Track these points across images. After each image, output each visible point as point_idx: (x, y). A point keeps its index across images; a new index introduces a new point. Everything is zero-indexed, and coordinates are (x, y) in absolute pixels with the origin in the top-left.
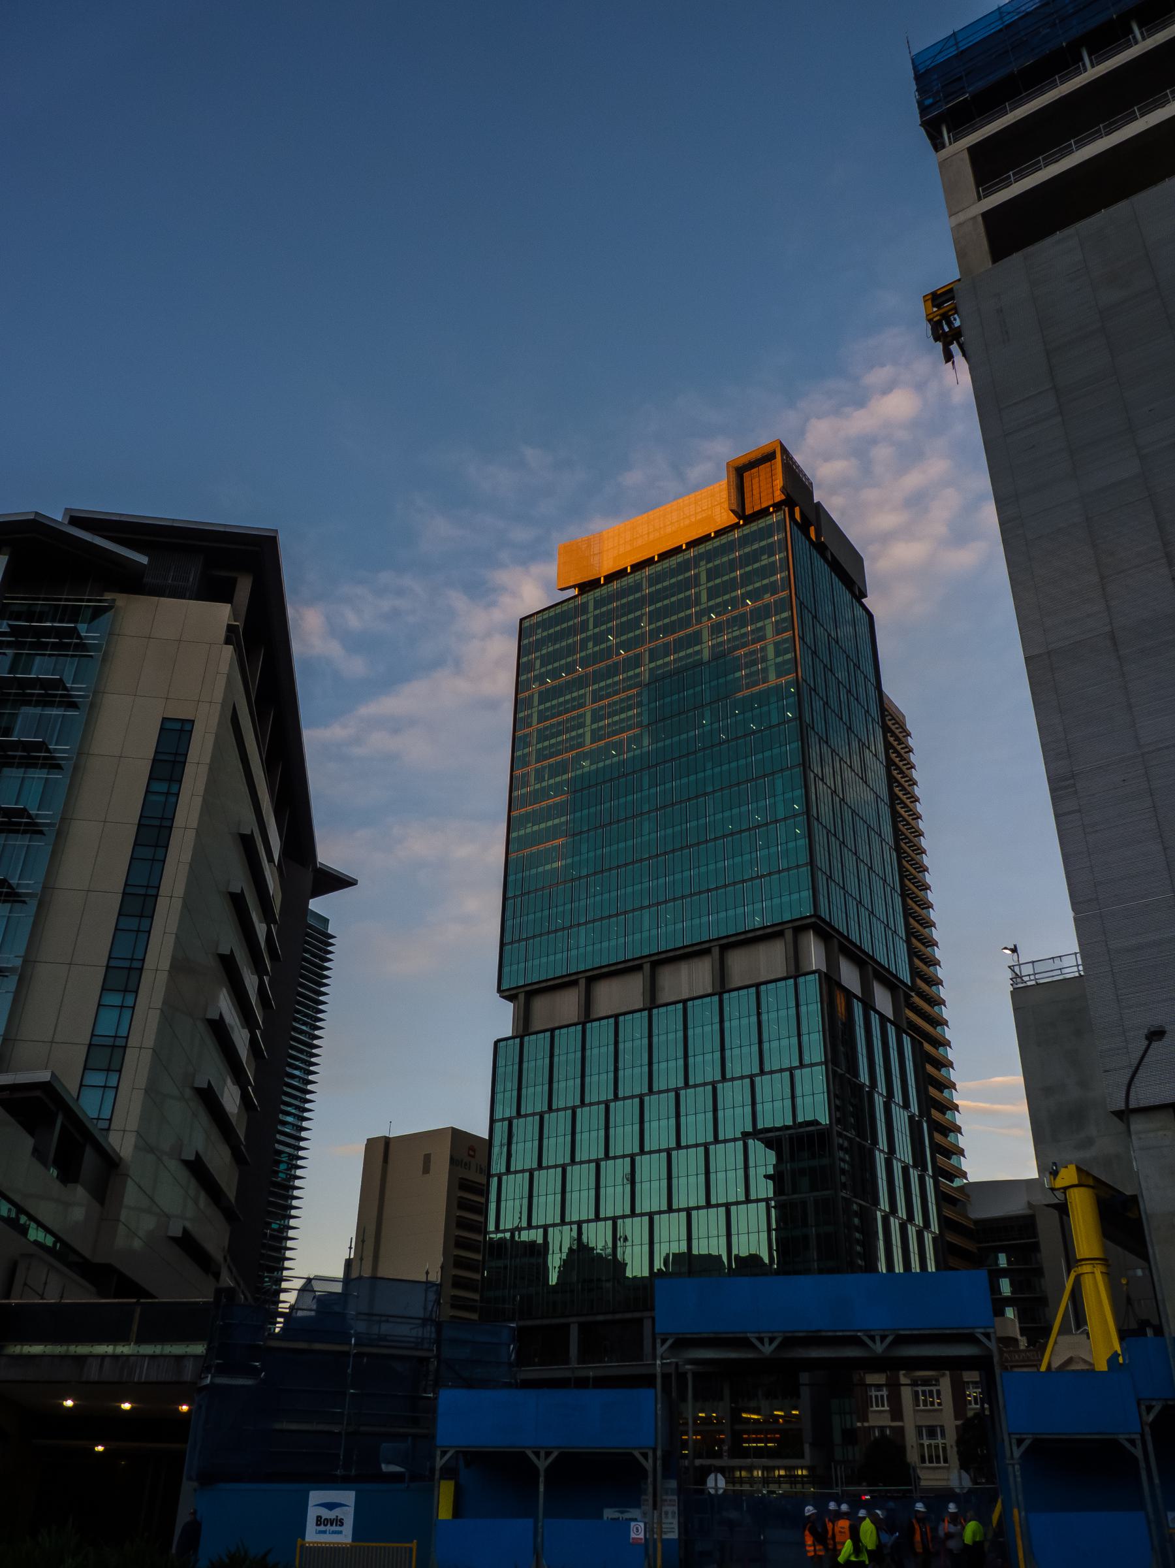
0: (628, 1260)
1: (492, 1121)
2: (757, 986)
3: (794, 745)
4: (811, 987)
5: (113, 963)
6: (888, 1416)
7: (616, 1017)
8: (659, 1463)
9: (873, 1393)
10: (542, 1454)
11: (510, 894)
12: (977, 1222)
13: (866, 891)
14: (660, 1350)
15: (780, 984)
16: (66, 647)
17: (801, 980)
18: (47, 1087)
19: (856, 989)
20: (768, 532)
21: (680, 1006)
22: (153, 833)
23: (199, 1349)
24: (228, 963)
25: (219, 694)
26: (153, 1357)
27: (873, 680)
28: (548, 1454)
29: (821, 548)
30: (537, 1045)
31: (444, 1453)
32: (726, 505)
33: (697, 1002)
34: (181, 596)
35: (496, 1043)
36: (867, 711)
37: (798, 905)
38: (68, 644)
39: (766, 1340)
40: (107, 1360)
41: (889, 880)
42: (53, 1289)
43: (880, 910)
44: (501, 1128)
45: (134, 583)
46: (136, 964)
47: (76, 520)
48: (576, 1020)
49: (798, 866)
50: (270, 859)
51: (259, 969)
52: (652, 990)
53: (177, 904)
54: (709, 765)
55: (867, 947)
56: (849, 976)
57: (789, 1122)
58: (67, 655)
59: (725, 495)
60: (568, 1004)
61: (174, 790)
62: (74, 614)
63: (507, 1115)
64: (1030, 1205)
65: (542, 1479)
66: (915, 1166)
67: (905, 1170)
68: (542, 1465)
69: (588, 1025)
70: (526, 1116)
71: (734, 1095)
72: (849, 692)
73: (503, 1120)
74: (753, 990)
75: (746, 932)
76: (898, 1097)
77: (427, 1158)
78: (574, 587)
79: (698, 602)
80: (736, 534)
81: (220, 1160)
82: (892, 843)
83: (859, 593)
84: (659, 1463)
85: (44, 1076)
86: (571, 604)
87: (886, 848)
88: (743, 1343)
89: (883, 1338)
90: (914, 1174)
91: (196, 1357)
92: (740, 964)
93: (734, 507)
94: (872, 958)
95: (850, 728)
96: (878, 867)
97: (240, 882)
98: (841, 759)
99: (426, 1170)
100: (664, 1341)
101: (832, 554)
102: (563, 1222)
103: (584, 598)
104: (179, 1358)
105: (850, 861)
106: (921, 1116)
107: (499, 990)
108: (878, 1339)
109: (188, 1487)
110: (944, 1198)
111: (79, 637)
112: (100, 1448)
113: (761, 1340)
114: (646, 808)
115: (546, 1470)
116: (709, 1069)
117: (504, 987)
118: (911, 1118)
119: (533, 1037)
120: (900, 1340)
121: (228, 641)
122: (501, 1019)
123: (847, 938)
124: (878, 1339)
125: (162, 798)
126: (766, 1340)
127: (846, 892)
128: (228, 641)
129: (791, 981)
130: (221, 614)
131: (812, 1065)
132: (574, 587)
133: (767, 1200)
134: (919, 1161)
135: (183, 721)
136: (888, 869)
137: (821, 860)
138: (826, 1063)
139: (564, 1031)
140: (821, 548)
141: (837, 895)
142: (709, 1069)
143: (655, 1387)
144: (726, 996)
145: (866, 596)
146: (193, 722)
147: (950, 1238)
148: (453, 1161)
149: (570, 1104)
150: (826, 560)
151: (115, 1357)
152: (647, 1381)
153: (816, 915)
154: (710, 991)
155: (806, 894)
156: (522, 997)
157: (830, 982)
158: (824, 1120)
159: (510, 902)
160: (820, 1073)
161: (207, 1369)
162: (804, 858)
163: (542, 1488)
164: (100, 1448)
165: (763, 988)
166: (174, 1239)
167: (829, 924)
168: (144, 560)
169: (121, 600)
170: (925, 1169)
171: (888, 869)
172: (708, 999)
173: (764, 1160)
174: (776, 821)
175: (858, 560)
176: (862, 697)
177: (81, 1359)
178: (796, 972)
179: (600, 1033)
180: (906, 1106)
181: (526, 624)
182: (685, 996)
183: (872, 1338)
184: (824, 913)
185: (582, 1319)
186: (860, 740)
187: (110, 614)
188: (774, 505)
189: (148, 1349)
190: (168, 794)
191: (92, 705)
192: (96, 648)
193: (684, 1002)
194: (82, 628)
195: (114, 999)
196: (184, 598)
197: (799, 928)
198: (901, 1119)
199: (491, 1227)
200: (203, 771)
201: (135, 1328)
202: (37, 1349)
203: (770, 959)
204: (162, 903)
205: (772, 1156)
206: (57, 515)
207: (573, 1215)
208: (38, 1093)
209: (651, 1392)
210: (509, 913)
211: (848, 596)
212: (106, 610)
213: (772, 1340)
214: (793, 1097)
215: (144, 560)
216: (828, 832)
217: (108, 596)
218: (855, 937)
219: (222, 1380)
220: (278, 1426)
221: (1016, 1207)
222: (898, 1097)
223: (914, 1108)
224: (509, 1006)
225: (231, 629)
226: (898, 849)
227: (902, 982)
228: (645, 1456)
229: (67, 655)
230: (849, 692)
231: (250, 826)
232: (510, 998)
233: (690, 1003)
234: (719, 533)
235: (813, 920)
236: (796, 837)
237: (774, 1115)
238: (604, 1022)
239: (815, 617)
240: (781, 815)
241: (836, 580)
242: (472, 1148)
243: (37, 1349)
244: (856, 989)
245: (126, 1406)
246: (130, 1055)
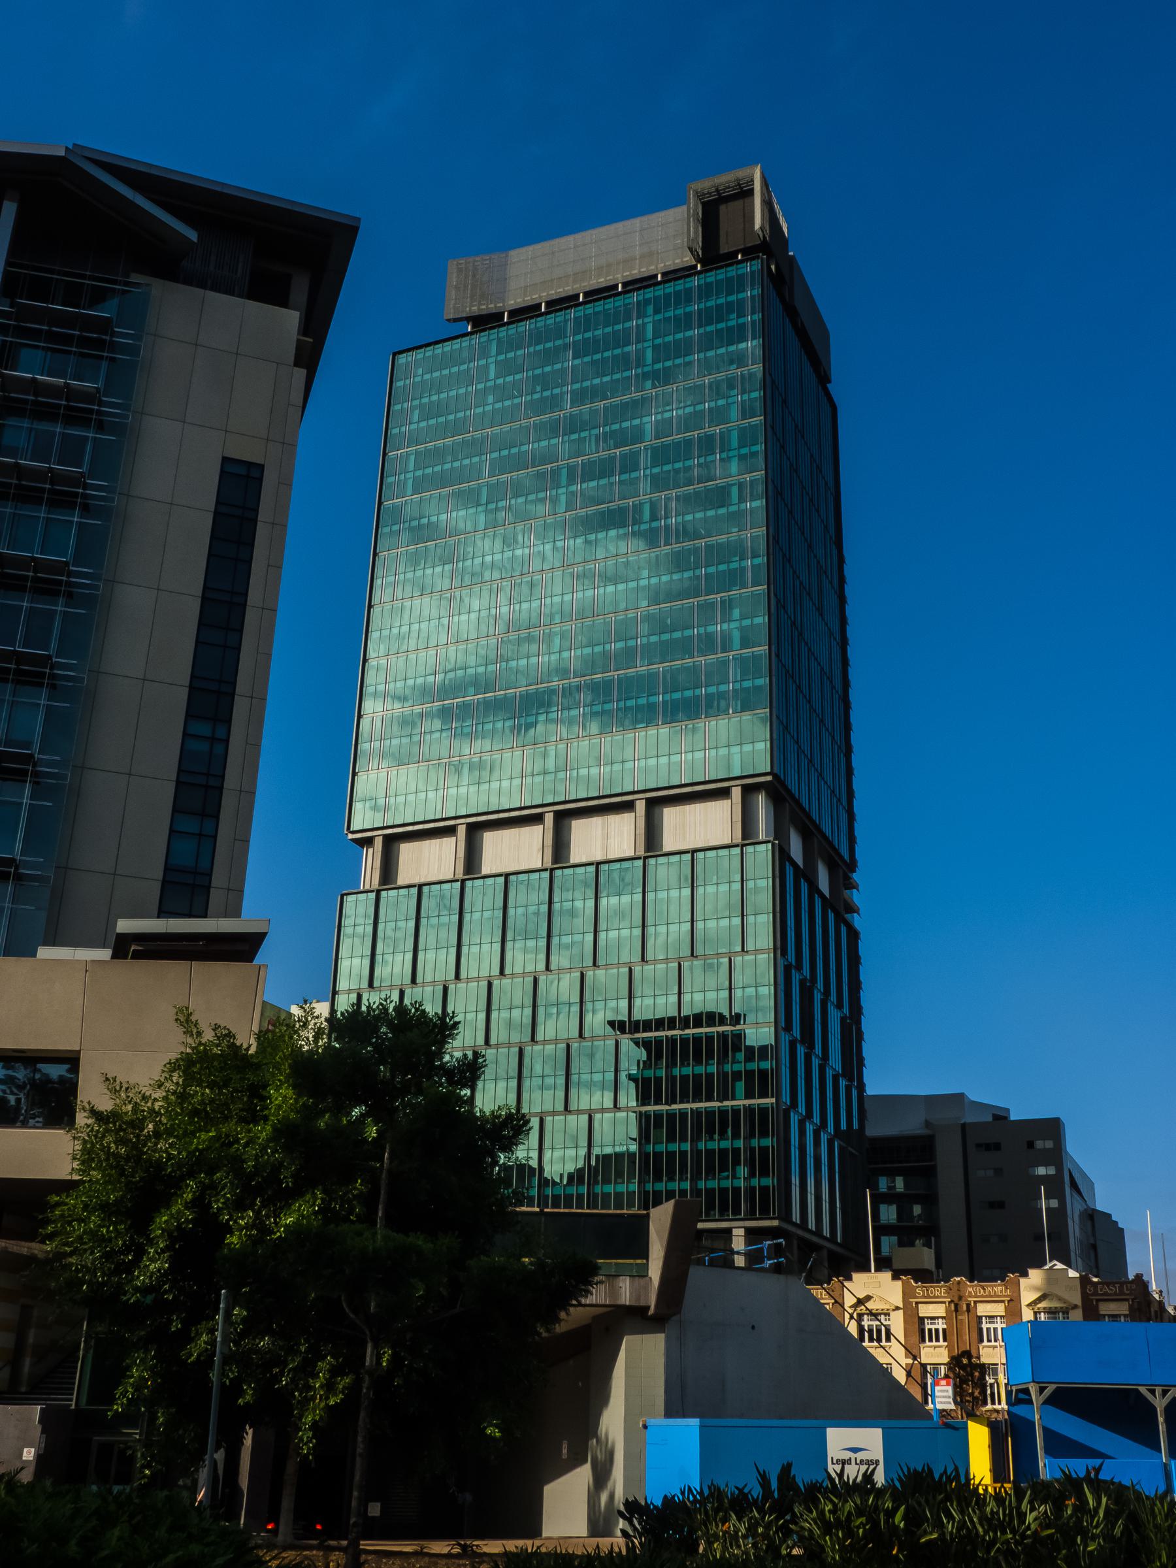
12: (874, 1140)
20: (736, 285)
29: (791, 311)
34: (230, 292)
36: (826, 527)
38: (94, 343)
41: (837, 737)
45: (170, 264)
48: (450, 876)
55: (815, 816)
58: (37, 347)
64: (928, 1124)
67: (836, 1078)
72: (811, 500)
74: (689, 856)
76: (833, 997)
79: (640, 362)
80: (696, 281)
83: (824, 379)
87: (836, 697)
90: (843, 1083)
98: (801, 583)
103: (483, 337)
111: (113, 334)
115: (1168, 1409)
118: (843, 1019)
121: (297, 364)
123: (797, 802)
128: (297, 364)
129: (737, 851)
132: (468, 319)
140: (791, 311)
145: (830, 382)
146: (261, 467)
157: (782, 856)
160: (765, 960)
165: (700, 855)
168: (193, 235)
169: (158, 288)
173: (632, 1055)
180: (839, 1006)
181: (402, 359)
182: (599, 858)
188: (745, 252)
198: (834, 1016)
215: (193, 235)
217: (135, 278)
221: (910, 1125)
222: (833, 997)
223: (846, 1010)
227: (841, 858)
229: (37, 347)
234: (671, 276)
235: (769, 778)
238: (490, 881)
239: (784, 402)
241: (804, 358)
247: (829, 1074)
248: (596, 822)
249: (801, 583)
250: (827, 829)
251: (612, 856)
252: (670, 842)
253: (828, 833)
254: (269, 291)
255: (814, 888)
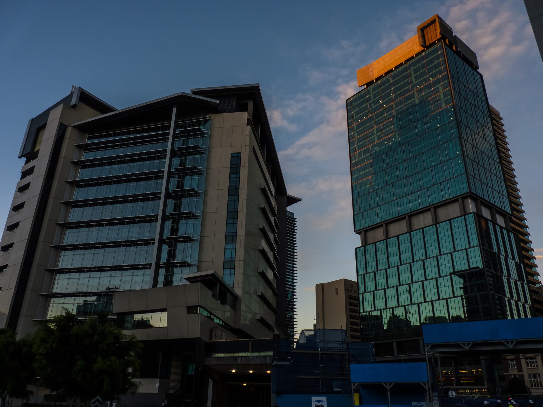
0: (411, 320)
1: (358, 276)
2: (450, 220)
3: (455, 130)
4: (471, 219)
5: (227, 235)
6: (517, 370)
7: (398, 236)
8: (430, 387)
9: (510, 363)
10: (388, 384)
11: (355, 198)
13: (489, 180)
14: (426, 349)
15: (458, 219)
16: (198, 135)
17: (467, 216)
18: (213, 275)
19: (489, 217)
20: (436, 50)
21: (421, 230)
22: (234, 191)
23: (271, 353)
24: (263, 231)
25: (248, 143)
26: (257, 356)
27: (484, 100)
28: (390, 385)
29: (458, 53)
30: (370, 249)
31: (354, 385)
32: (418, 44)
33: (428, 228)
35: (356, 249)
36: (483, 113)
37: (462, 188)
39: (466, 345)
40: (243, 358)
41: (499, 176)
42: (224, 337)
43: (496, 188)
44: (361, 278)
45: (215, 110)
46: (234, 234)
47: (195, 93)
49: (461, 175)
50: (272, 195)
51: (273, 232)
52: (410, 225)
53: (244, 213)
54: (422, 142)
56: (486, 213)
57: (468, 268)
59: (417, 40)
60: (380, 233)
61: (238, 176)
62: (199, 123)
63: (363, 273)
65: (389, 393)
66: (519, 281)
67: (516, 282)
68: (388, 388)
69: (388, 240)
70: (369, 273)
71: (445, 260)
72: (475, 106)
73: (361, 275)
74: (448, 222)
75: (443, 201)
76: (510, 256)
77: (337, 289)
78: (364, 85)
79: (411, 82)
80: (424, 54)
81: (269, 294)
82: (498, 160)
84: (430, 387)
85: (212, 272)
86: (364, 92)
87: (496, 164)
88: (458, 346)
89: (512, 342)
90: (519, 284)
91: (270, 356)
92: (442, 213)
93: (422, 44)
94: (494, 205)
95: (477, 120)
96: (493, 171)
97: (263, 204)
98: (474, 132)
99: (337, 293)
100: (427, 346)
101: (463, 55)
102: (387, 308)
104: (265, 357)
105: (482, 170)
106: (520, 262)
107: (355, 231)
108: (510, 342)
109: (273, 396)
110: (532, 291)
111: (201, 131)
112: (245, 385)
113: (464, 344)
114: (400, 161)
115: (391, 389)
116: (434, 251)
117: (357, 229)
118: (516, 263)
119: (369, 246)
120: (519, 343)
121: (248, 125)
122: (357, 241)
124: (510, 342)
125: (235, 180)
126: (466, 345)
127: (481, 182)
128: (248, 125)
129: (463, 217)
130: (245, 115)
131: (474, 247)
132: (364, 85)
133: (461, 296)
134: (521, 278)
135: (238, 153)
136: (498, 171)
137: (470, 171)
138: (480, 245)
139: (379, 243)
140: (458, 53)
141: (478, 183)
142: (434, 251)
143: (426, 361)
144: (438, 225)
145: (478, 68)
146: (241, 153)
147: (536, 306)
148: (346, 290)
149: (384, 268)
150: (460, 57)
151: (245, 357)
152: (424, 360)
153: (470, 192)
154: (432, 224)
155: (466, 185)
156: (363, 233)
157: (478, 216)
158: (481, 266)
159: (355, 200)
160: (477, 250)
161: (274, 360)
162: (463, 171)
163: (389, 395)
164: (245, 385)
166: (258, 320)
167: (476, 195)
168: (218, 102)
169: (212, 116)
170: (523, 281)
171: (498, 171)
172: (431, 227)
173: (459, 282)
174: (451, 159)
175: (474, 55)
176: (481, 108)
177: (235, 358)
178: (464, 213)
179: (393, 243)
180: (514, 258)
182: (423, 226)
183: (508, 342)
184: (473, 191)
185: (397, 340)
186: (481, 124)
187: (209, 123)
189: (255, 354)
190: (236, 178)
191: (209, 152)
192: (207, 133)
193: (423, 228)
194: (202, 128)
195: (229, 246)
196: (232, 112)
197: (464, 197)
198: (512, 264)
199: (362, 311)
200: (247, 169)
201: (250, 347)
202: (222, 355)
203: (454, 210)
204: (240, 214)
205: (462, 281)
206: (189, 92)
207: (390, 305)
208: (211, 277)
209: (424, 363)
210: (355, 204)
211: (471, 69)
212: (208, 120)
213: (468, 344)
214: (468, 259)
215: (218, 102)
216: (472, 160)
217: (208, 116)
218: (486, 198)
219: (278, 363)
220: (298, 377)
222: (510, 256)
223: (517, 259)
224: (359, 236)
225: (248, 120)
226: (501, 163)
227: (508, 213)
228: (425, 384)
230: (475, 106)
231: (264, 185)
232: (359, 233)
233: (425, 229)
234: (417, 55)
236: (459, 164)
237: (461, 265)
238: (393, 238)
239: (458, 80)
240: (452, 157)
241: (465, 64)
242: (351, 285)
243: (222, 355)
244: (489, 217)
245: (251, 372)
246: (237, 263)
247: (512, 282)
248: (421, 217)
249: (474, 132)
250: (498, 204)
251: (426, 225)
252: (442, 219)
253: (500, 206)
254: (242, 108)
255: (495, 223)
